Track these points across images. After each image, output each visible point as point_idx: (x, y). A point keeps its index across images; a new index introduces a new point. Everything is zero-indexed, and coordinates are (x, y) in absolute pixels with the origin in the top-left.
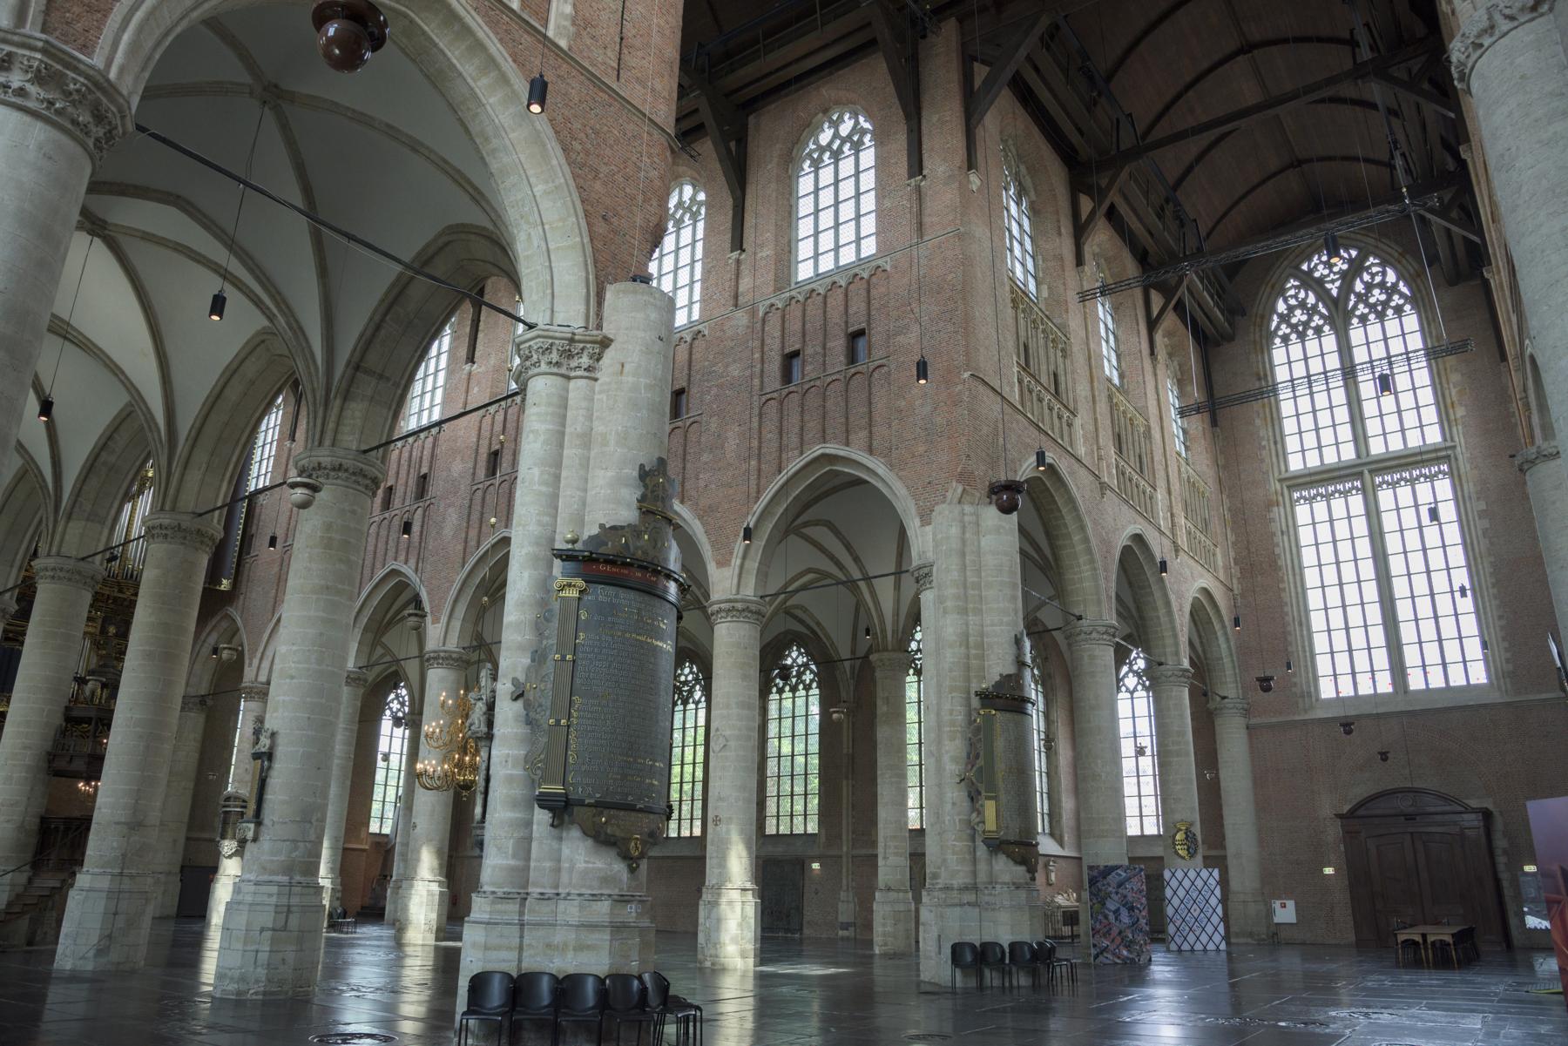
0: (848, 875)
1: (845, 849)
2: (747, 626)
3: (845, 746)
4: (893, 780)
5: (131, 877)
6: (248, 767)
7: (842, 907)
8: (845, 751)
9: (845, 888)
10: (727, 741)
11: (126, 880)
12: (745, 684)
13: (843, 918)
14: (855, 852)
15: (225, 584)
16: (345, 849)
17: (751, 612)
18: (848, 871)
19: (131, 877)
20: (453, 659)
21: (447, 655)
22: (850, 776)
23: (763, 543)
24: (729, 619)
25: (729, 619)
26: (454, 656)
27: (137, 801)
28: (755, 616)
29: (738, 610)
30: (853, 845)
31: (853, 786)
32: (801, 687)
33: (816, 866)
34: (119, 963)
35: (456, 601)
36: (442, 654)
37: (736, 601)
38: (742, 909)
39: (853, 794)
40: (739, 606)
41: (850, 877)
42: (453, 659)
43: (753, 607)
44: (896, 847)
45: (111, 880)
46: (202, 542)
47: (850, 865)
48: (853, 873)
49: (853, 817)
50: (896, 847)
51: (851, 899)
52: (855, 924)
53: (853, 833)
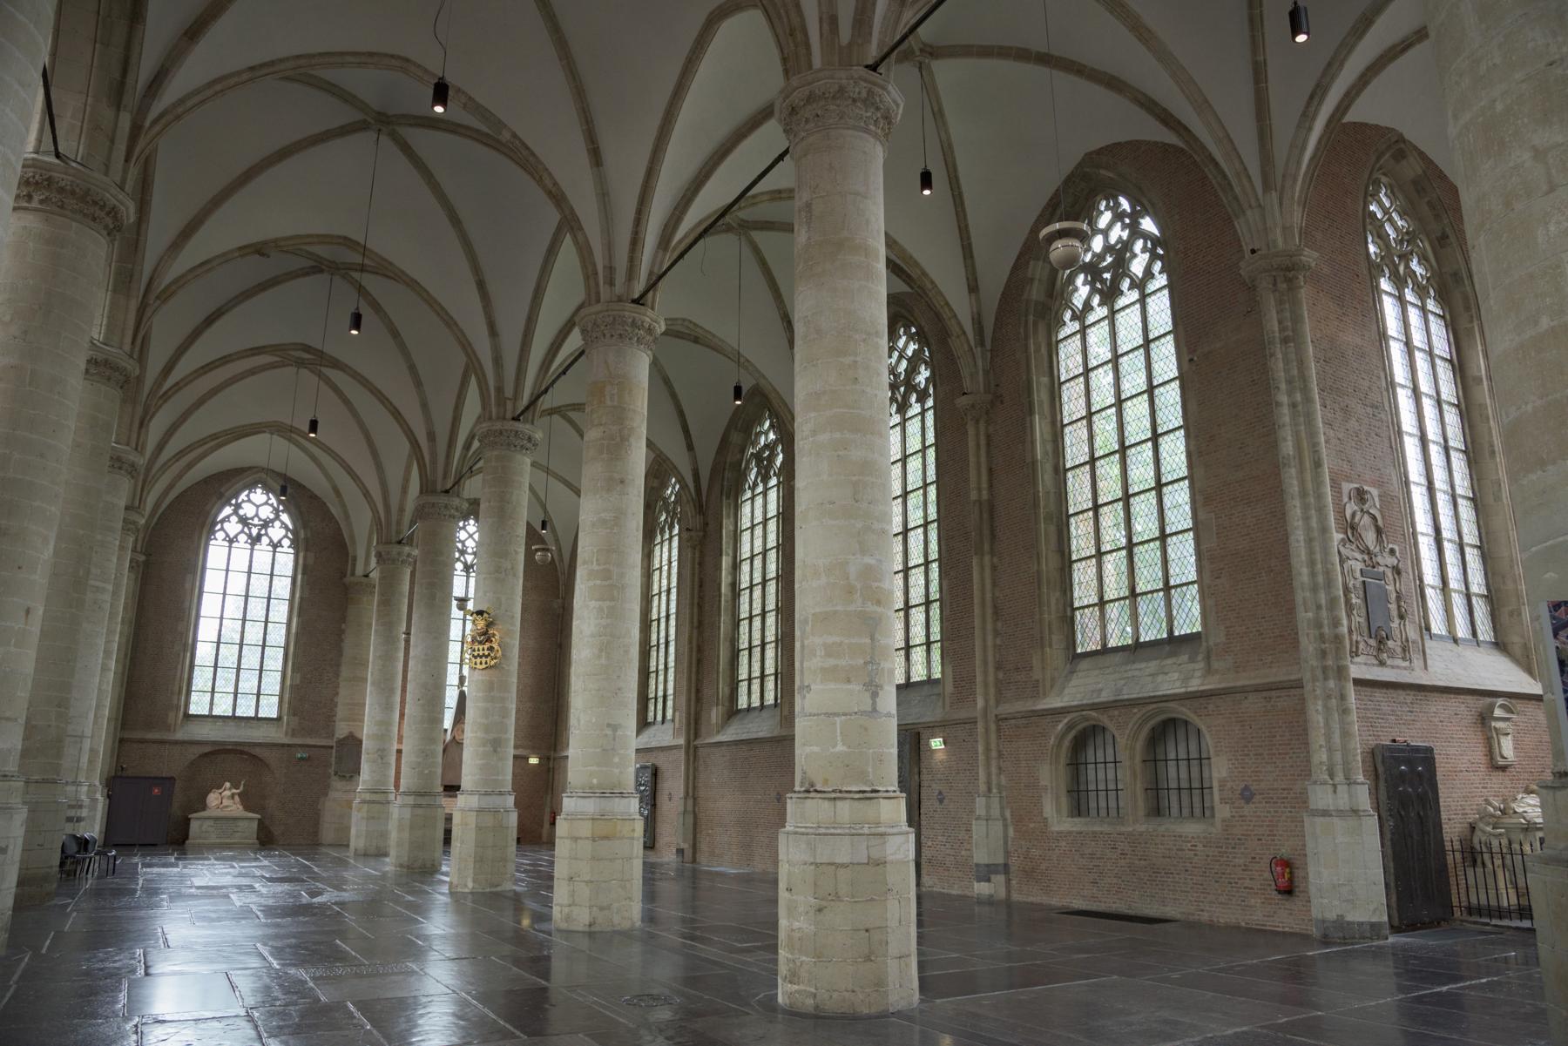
0: (988, 759)
1: (980, 703)
3: (973, 484)
4: (824, 437)
7: (978, 829)
8: (974, 496)
9: (983, 787)
13: (981, 857)
14: (1007, 709)
16: (122, 741)
18: (987, 750)
22: (987, 547)
30: (999, 692)
31: (994, 568)
32: (914, 398)
33: (937, 743)
39: (994, 584)
41: (994, 763)
44: (830, 651)
47: (993, 736)
48: (1000, 755)
49: (996, 633)
50: (830, 651)
51: (996, 812)
52: (1006, 869)
53: (999, 667)
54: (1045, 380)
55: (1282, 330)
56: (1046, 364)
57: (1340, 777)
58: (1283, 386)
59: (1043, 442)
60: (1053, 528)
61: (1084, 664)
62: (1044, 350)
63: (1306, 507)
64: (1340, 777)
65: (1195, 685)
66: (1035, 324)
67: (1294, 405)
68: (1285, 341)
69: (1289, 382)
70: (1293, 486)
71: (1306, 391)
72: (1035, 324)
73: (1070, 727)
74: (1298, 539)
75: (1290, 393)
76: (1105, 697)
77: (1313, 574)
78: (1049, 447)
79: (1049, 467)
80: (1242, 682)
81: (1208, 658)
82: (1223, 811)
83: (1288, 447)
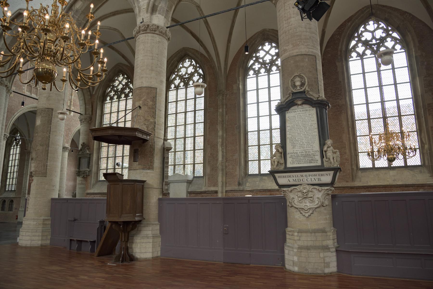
54: (8, 154)
55: (27, 159)
56: (9, 152)
57: (23, 207)
58: (26, 165)
59: (6, 162)
60: (5, 174)
61: (6, 192)
62: (9, 150)
63: (25, 179)
64: (23, 207)
65: (14, 196)
66: (8, 146)
67: (26, 168)
68: (27, 160)
69: (26, 165)
70: (24, 177)
71: (28, 166)
72: (8, 146)
73: (2, 200)
74: (24, 182)
75: (26, 166)
76: (6, 197)
77: (24, 186)
78: (7, 163)
79: (6, 166)
80: (17, 197)
81: (16, 193)
82: (14, 210)
83: (25, 172)
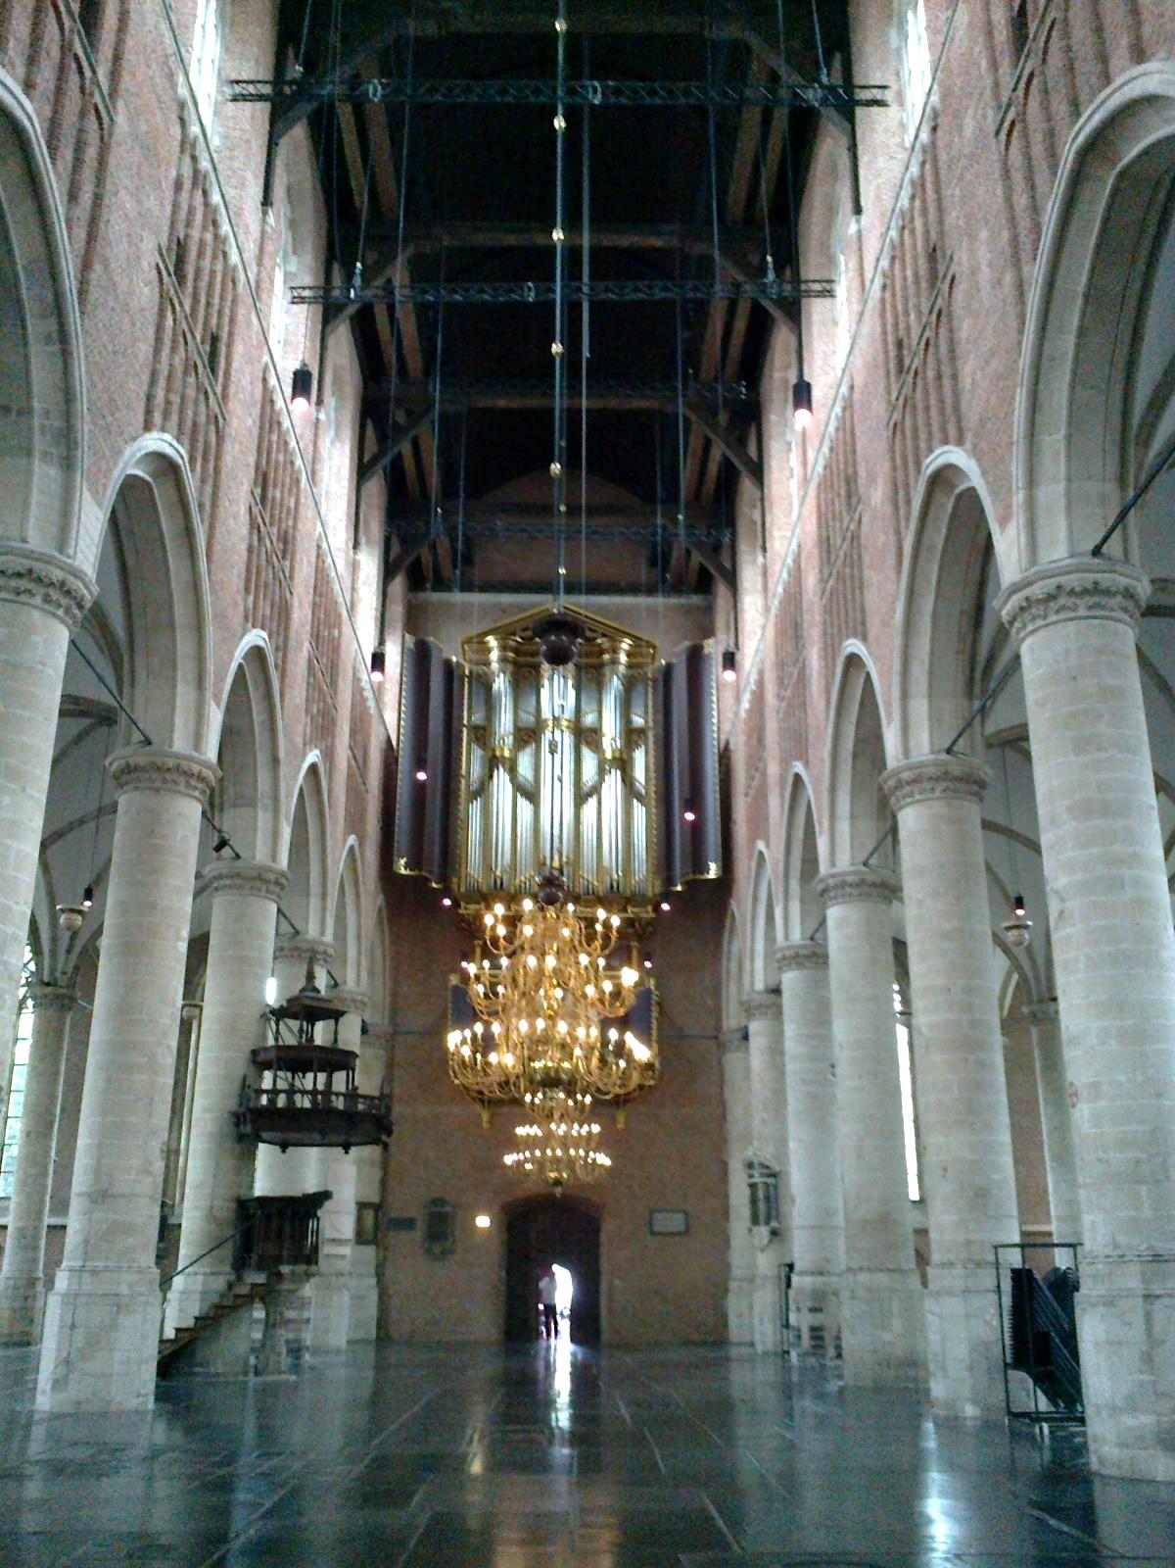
2: (1071, 627)
5: (94, 1272)
6: (765, 1116)
10: (1063, 900)
11: (86, 1277)
12: (1086, 758)
15: (713, 871)
17: (1072, 593)
19: (94, 1272)
20: (850, 885)
21: (837, 880)
23: (1063, 432)
24: (1030, 628)
25: (1030, 628)
26: (850, 879)
27: (98, 1160)
28: (1090, 600)
29: (1038, 601)
34: (79, 1403)
35: (833, 790)
36: (831, 882)
37: (1028, 583)
38: (1148, 1318)
40: (1037, 590)
42: (850, 885)
43: (1071, 581)
45: (70, 1278)
46: (164, 780)
